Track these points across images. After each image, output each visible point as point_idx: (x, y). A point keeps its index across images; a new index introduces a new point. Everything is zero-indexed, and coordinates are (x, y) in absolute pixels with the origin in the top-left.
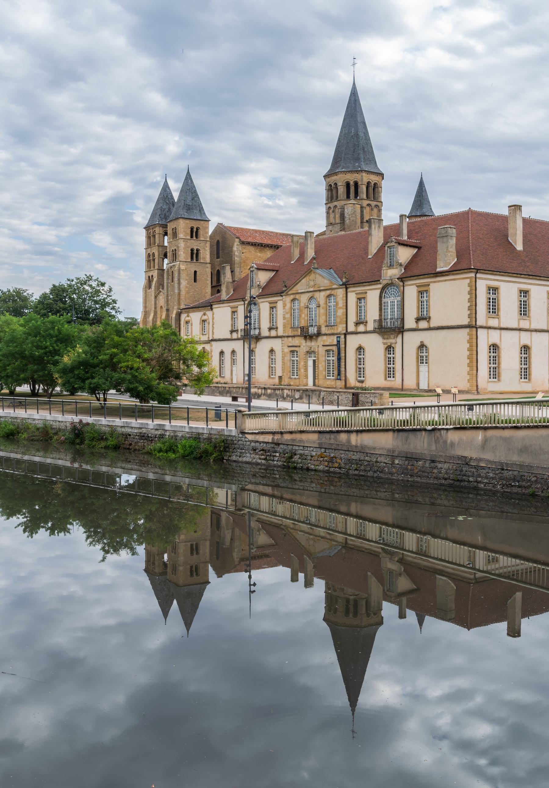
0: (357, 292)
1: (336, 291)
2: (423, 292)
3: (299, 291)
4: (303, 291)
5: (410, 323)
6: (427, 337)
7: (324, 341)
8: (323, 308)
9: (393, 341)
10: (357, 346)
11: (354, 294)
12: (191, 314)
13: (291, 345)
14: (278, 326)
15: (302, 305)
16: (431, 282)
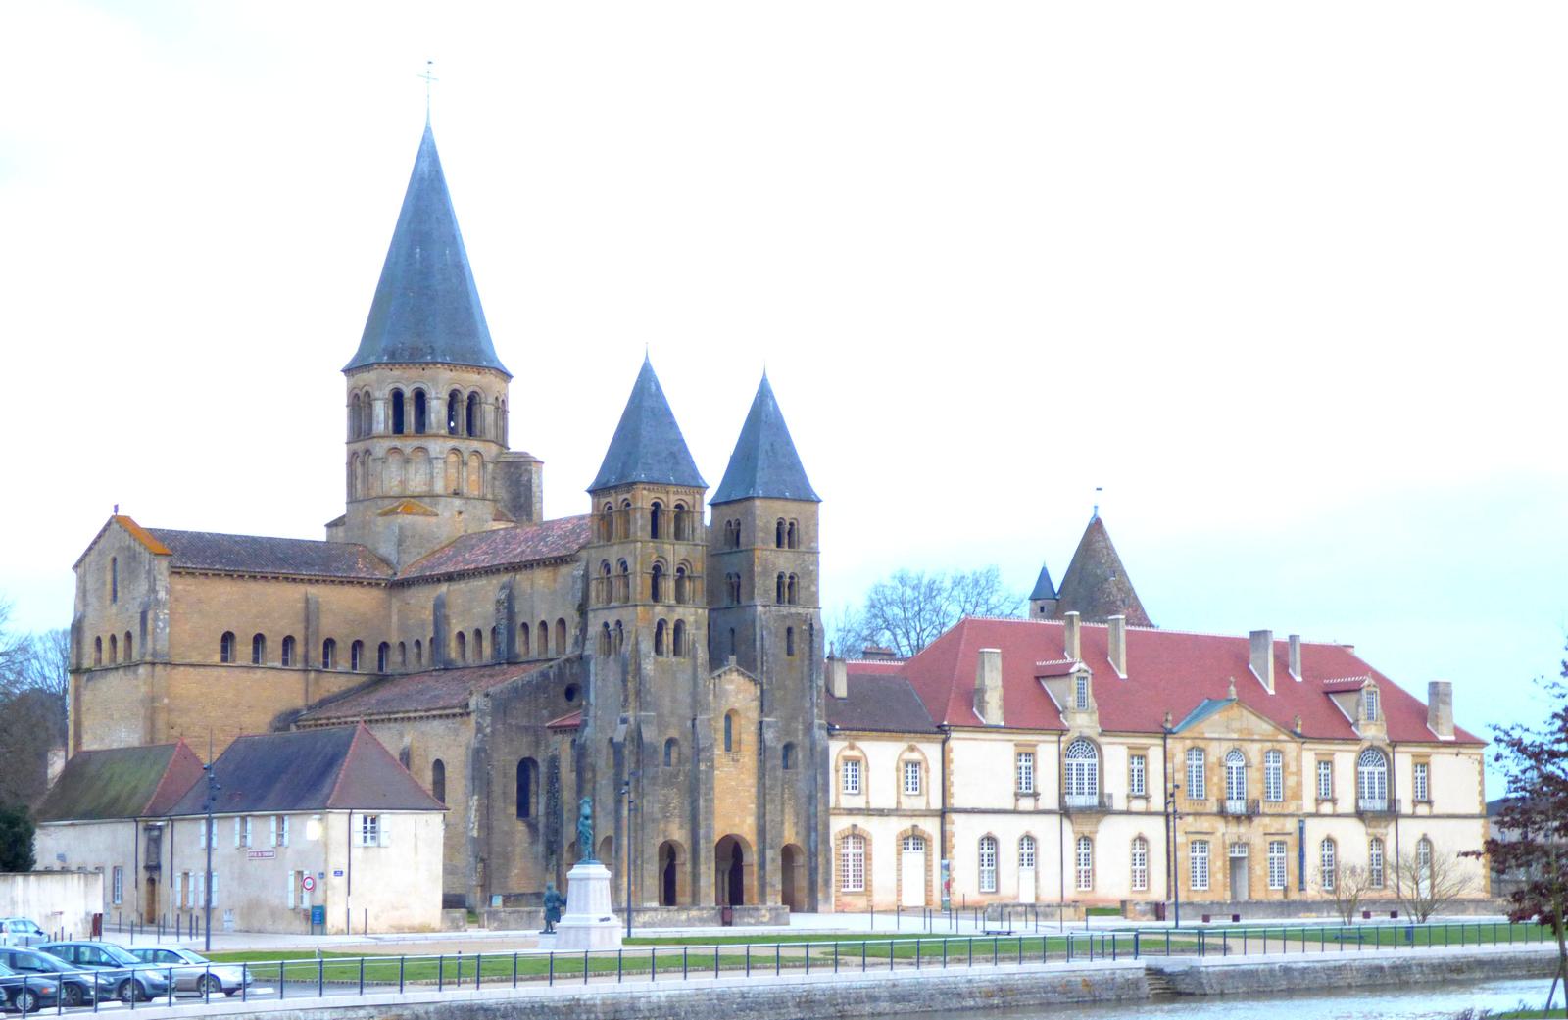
0: (1317, 751)
1: (1284, 744)
2: (1422, 765)
3: (1207, 735)
4: (1216, 735)
5: (1406, 807)
6: (1432, 828)
7: (1266, 826)
8: (1258, 770)
9: (1384, 831)
10: (1323, 836)
11: (1313, 752)
12: (862, 744)
13: (1193, 830)
14: (1151, 791)
15: (1213, 759)
16: (1437, 753)
